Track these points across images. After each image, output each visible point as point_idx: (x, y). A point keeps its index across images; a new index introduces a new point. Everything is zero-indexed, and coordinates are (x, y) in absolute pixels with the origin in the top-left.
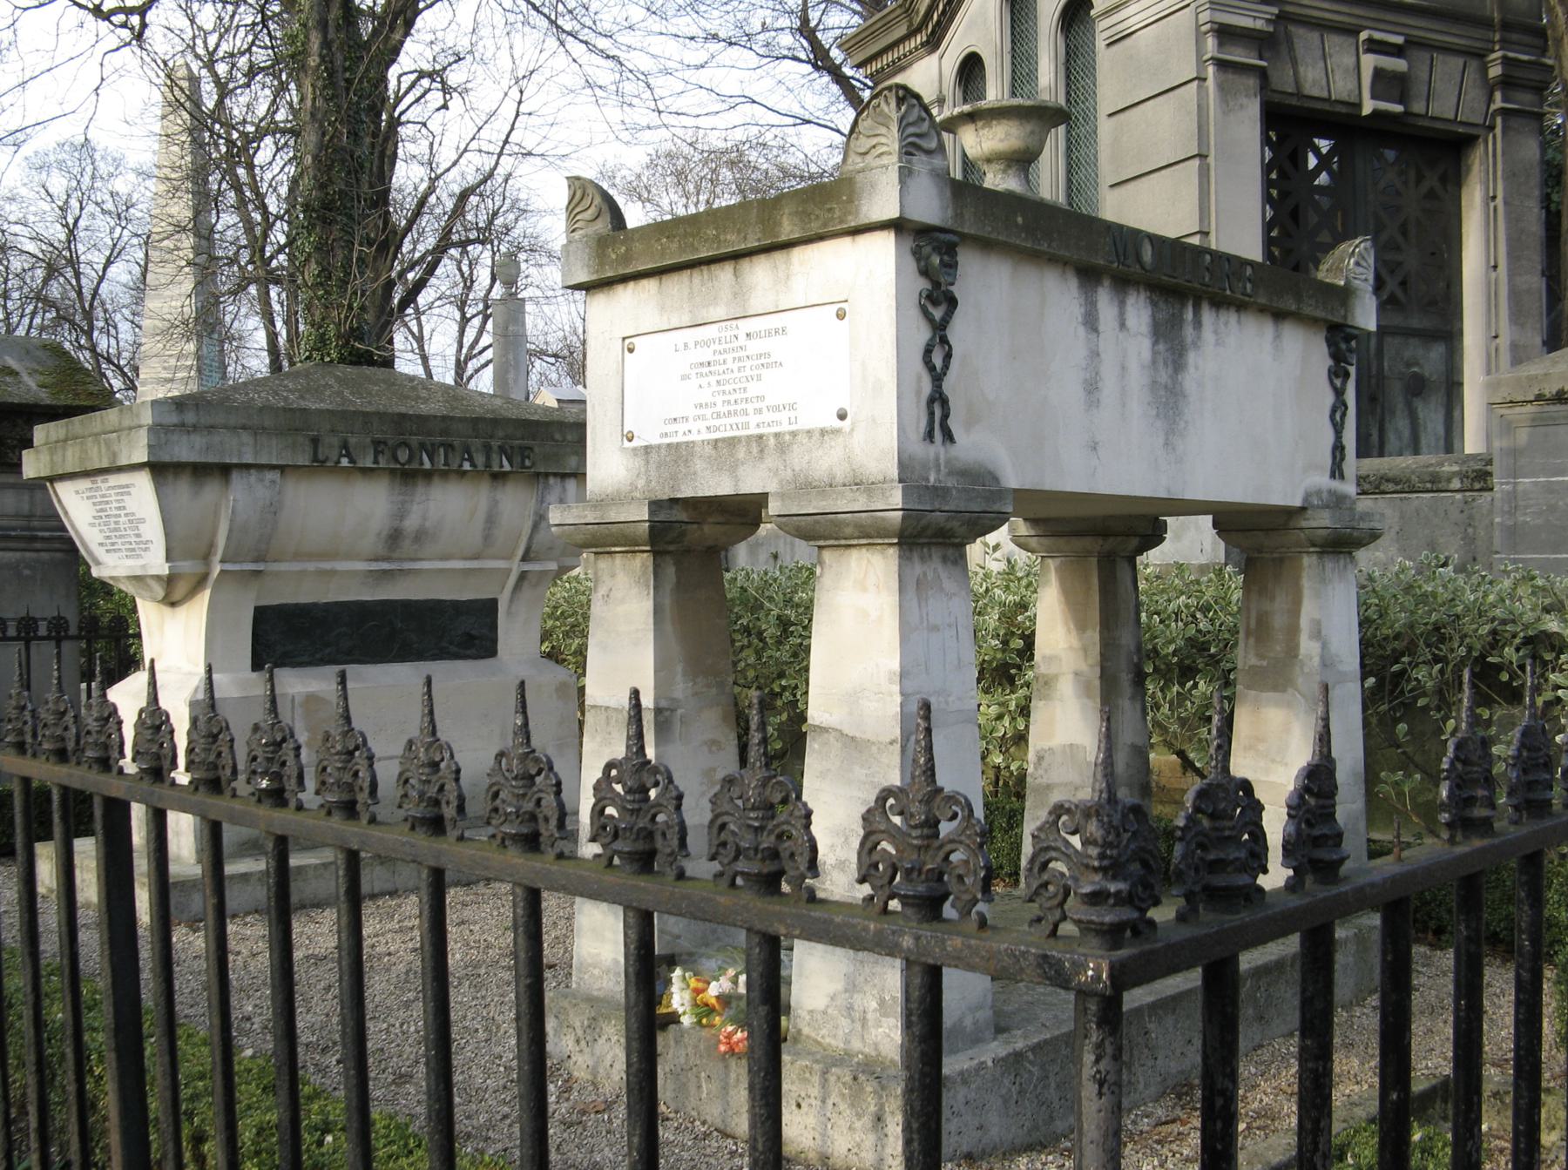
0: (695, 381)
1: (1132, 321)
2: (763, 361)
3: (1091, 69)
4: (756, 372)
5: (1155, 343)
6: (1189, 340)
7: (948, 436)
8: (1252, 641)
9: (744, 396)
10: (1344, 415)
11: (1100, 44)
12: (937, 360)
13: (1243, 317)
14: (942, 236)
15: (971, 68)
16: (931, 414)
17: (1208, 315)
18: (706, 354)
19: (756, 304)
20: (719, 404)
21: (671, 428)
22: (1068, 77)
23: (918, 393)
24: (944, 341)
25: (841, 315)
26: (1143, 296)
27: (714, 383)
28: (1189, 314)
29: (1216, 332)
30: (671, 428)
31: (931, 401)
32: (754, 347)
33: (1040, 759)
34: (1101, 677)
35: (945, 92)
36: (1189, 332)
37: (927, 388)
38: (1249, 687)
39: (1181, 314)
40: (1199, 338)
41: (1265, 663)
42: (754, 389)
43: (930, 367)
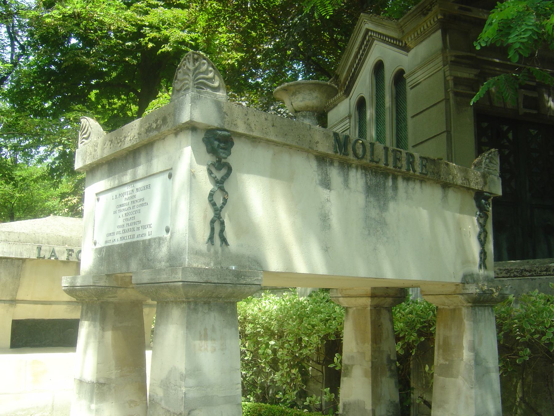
1: (352, 184)
2: (141, 203)
3: (405, 99)
4: (139, 208)
5: (367, 197)
6: (390, 196)
7: (224, 240)
8: (441, 351)
9: (134, 221)
10: (486, 236)
11: (408, 88)
12: (219, 201)
13: (424, 186)
14: (219, 132)
15: (361, 104)
16: (213, 229)
17: (401, 184)
20: (125, 225)
21: (110, 238)
22: (397, 104)
23: (205, 217)
24: (222, 189)
25: (170, 176)
26: (360, 172)
27: (124, 215)
28: (390, 183)
29: (406, 192)
30: (110, 238)
31: (212, 222)
33: (344, 405)
34: (372, 367)
35: (351, 113)
36: (390, 192)
37: (211, 214)
38: (440, 375)
39: (384, 183)
40: (396, 195)
41: (447, 363)
43: (214, 204)
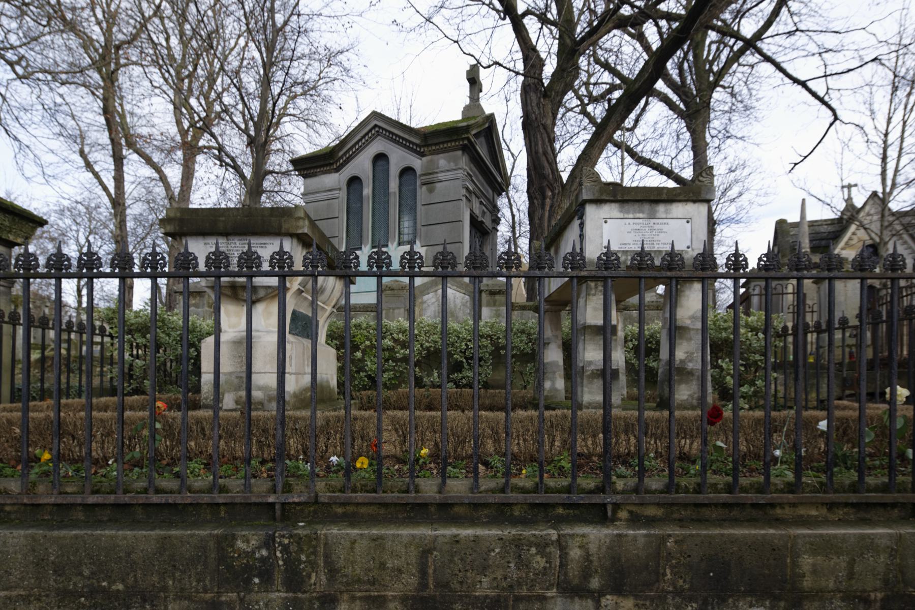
0: (633, 234)
18: (638, 227)
19: (658, 215)
32: (656, 227)
42: (656, 238)
